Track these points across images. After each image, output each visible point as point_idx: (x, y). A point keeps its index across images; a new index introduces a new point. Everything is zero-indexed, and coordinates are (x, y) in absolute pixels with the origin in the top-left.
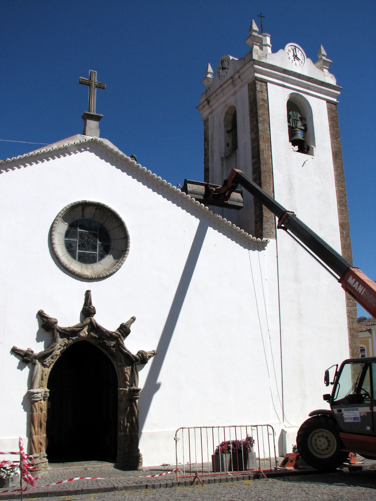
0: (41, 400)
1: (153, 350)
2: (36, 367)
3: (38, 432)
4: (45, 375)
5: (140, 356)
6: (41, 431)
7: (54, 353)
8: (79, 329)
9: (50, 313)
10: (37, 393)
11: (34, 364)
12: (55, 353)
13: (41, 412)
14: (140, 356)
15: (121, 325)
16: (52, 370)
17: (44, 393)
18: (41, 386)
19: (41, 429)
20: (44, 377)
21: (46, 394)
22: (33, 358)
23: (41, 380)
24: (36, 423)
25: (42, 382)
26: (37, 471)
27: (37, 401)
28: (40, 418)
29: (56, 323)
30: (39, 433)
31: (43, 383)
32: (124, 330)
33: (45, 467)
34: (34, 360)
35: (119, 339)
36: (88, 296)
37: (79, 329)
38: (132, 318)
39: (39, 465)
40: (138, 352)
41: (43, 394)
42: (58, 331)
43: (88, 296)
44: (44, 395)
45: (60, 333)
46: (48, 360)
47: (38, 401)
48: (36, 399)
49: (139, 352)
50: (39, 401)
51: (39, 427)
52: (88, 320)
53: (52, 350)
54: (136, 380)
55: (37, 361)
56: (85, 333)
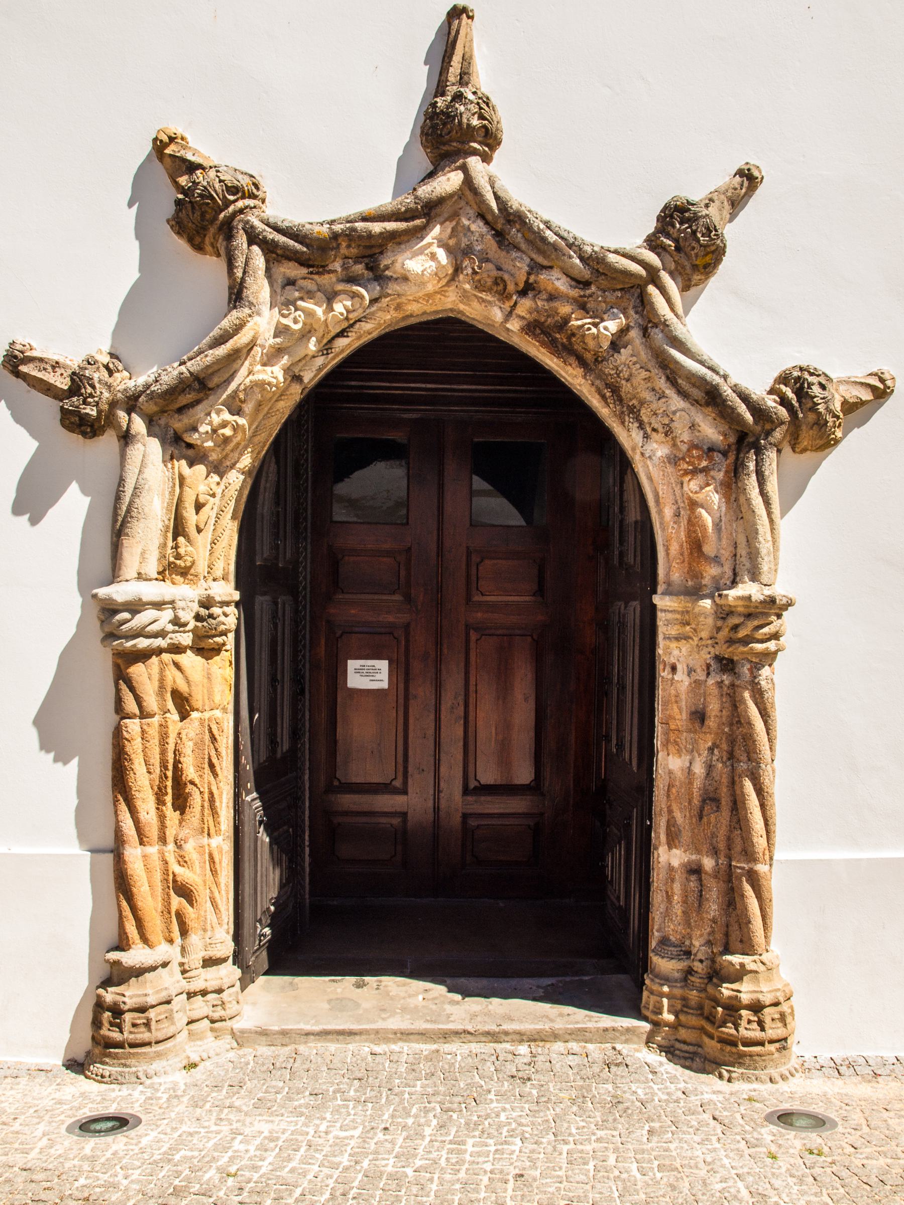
0: (177, 649)
1: (875, 370)
2: (135, 452)
3: (163, 827)
4: (199, 506)
5: (790, 394)
6: (181, 822)
7: (242, 379)
8: (391, 226)
9: (218, 151)
10: (135, 607)
11: (126, 438)
12: (250, 372)
13: (184, 716)
14: (790, 394)
15: (666, 207)
16: (257, 477)
17: (196, 607)
18: (174, 569)
19: (182, 813)
20: (191, 517)
21: (211, 616)
22: (113, 404)
23: (175, 539)
24: (142, 781)
25: (176, 547)
26: (149, 1044)
27: (143, 656)
28: (171, 747)
29: (253, 192)
30: (170, 833)
31: (182, 551)
32: (688, 241)
33: (216, 1016)
34: (122, 415)
35: (651, 289)
36: (453, 33)
37: (391, 226)
38: (740, 173)
39: (152, 1014)
40: (776, 374)
41: (187, 616)
42: (253, 238)
43: (453, 33)
44: (198, 618)
45: (271, 250)
46: (214, 420)
47: (159, 651)
48: (142, 643)
49: (784, 379)
50: (166, 657)
51: (169, 799)
52: (449, 181)
53: (221, 351)
54: (764, 545)
55: (139, 425)
56: (433, 256)
